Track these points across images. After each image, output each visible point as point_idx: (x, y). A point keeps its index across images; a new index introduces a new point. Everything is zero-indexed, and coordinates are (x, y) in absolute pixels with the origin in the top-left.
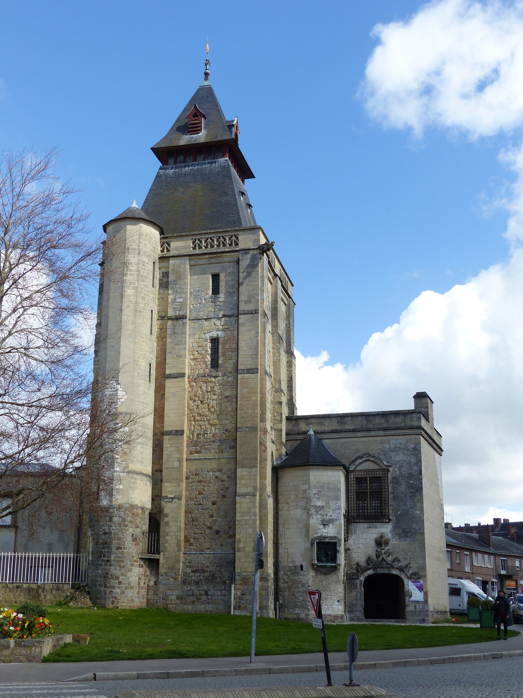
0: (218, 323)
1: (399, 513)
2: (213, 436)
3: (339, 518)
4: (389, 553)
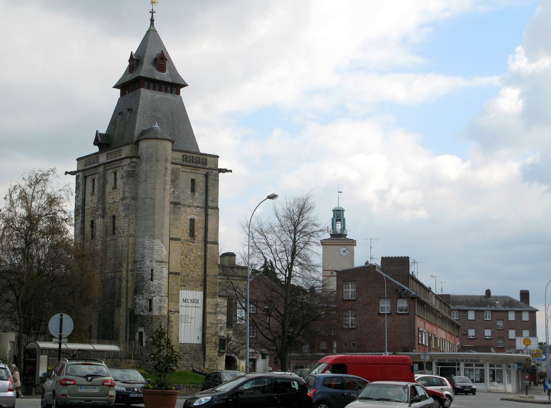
0: (194, 210)
2: (192, 277)
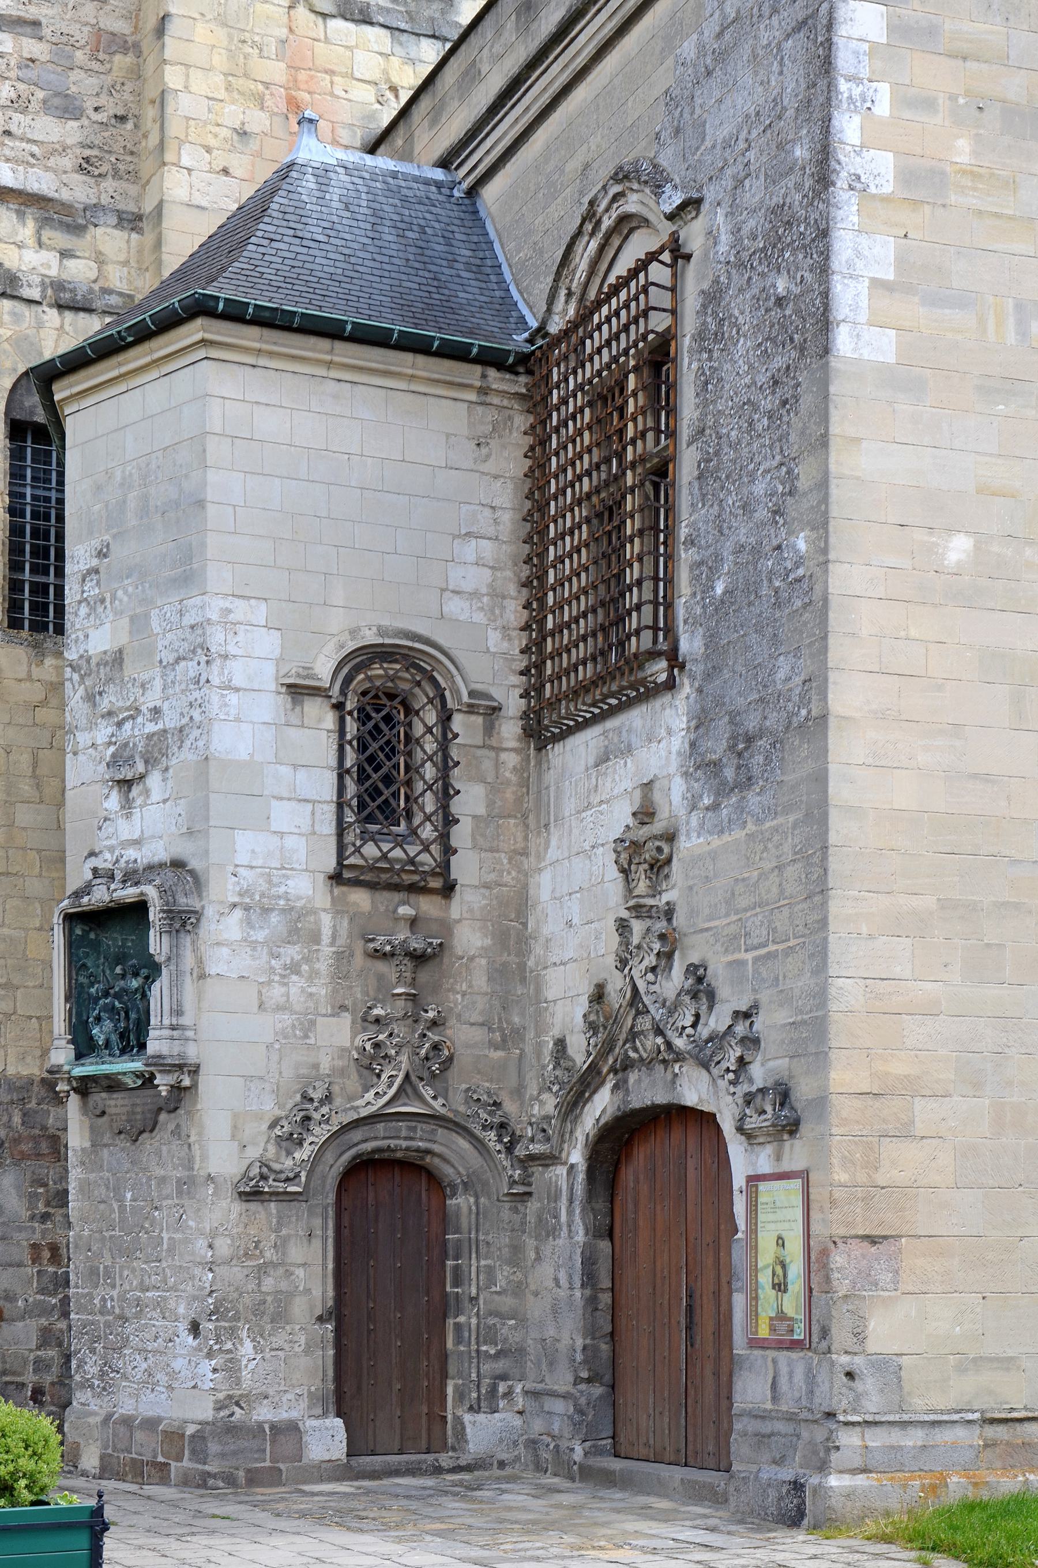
1: (719, 589)
3: (196, 714)
4: (662, 937)
